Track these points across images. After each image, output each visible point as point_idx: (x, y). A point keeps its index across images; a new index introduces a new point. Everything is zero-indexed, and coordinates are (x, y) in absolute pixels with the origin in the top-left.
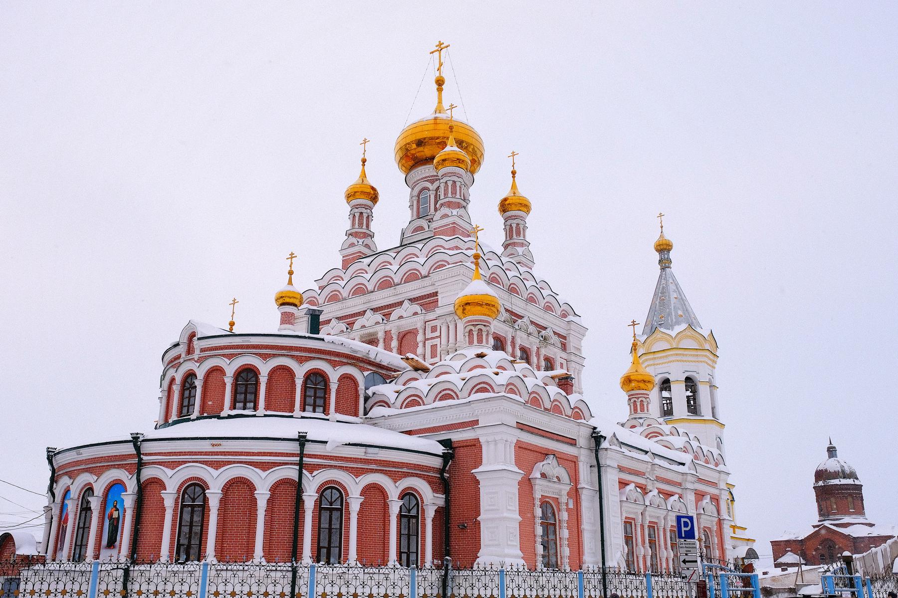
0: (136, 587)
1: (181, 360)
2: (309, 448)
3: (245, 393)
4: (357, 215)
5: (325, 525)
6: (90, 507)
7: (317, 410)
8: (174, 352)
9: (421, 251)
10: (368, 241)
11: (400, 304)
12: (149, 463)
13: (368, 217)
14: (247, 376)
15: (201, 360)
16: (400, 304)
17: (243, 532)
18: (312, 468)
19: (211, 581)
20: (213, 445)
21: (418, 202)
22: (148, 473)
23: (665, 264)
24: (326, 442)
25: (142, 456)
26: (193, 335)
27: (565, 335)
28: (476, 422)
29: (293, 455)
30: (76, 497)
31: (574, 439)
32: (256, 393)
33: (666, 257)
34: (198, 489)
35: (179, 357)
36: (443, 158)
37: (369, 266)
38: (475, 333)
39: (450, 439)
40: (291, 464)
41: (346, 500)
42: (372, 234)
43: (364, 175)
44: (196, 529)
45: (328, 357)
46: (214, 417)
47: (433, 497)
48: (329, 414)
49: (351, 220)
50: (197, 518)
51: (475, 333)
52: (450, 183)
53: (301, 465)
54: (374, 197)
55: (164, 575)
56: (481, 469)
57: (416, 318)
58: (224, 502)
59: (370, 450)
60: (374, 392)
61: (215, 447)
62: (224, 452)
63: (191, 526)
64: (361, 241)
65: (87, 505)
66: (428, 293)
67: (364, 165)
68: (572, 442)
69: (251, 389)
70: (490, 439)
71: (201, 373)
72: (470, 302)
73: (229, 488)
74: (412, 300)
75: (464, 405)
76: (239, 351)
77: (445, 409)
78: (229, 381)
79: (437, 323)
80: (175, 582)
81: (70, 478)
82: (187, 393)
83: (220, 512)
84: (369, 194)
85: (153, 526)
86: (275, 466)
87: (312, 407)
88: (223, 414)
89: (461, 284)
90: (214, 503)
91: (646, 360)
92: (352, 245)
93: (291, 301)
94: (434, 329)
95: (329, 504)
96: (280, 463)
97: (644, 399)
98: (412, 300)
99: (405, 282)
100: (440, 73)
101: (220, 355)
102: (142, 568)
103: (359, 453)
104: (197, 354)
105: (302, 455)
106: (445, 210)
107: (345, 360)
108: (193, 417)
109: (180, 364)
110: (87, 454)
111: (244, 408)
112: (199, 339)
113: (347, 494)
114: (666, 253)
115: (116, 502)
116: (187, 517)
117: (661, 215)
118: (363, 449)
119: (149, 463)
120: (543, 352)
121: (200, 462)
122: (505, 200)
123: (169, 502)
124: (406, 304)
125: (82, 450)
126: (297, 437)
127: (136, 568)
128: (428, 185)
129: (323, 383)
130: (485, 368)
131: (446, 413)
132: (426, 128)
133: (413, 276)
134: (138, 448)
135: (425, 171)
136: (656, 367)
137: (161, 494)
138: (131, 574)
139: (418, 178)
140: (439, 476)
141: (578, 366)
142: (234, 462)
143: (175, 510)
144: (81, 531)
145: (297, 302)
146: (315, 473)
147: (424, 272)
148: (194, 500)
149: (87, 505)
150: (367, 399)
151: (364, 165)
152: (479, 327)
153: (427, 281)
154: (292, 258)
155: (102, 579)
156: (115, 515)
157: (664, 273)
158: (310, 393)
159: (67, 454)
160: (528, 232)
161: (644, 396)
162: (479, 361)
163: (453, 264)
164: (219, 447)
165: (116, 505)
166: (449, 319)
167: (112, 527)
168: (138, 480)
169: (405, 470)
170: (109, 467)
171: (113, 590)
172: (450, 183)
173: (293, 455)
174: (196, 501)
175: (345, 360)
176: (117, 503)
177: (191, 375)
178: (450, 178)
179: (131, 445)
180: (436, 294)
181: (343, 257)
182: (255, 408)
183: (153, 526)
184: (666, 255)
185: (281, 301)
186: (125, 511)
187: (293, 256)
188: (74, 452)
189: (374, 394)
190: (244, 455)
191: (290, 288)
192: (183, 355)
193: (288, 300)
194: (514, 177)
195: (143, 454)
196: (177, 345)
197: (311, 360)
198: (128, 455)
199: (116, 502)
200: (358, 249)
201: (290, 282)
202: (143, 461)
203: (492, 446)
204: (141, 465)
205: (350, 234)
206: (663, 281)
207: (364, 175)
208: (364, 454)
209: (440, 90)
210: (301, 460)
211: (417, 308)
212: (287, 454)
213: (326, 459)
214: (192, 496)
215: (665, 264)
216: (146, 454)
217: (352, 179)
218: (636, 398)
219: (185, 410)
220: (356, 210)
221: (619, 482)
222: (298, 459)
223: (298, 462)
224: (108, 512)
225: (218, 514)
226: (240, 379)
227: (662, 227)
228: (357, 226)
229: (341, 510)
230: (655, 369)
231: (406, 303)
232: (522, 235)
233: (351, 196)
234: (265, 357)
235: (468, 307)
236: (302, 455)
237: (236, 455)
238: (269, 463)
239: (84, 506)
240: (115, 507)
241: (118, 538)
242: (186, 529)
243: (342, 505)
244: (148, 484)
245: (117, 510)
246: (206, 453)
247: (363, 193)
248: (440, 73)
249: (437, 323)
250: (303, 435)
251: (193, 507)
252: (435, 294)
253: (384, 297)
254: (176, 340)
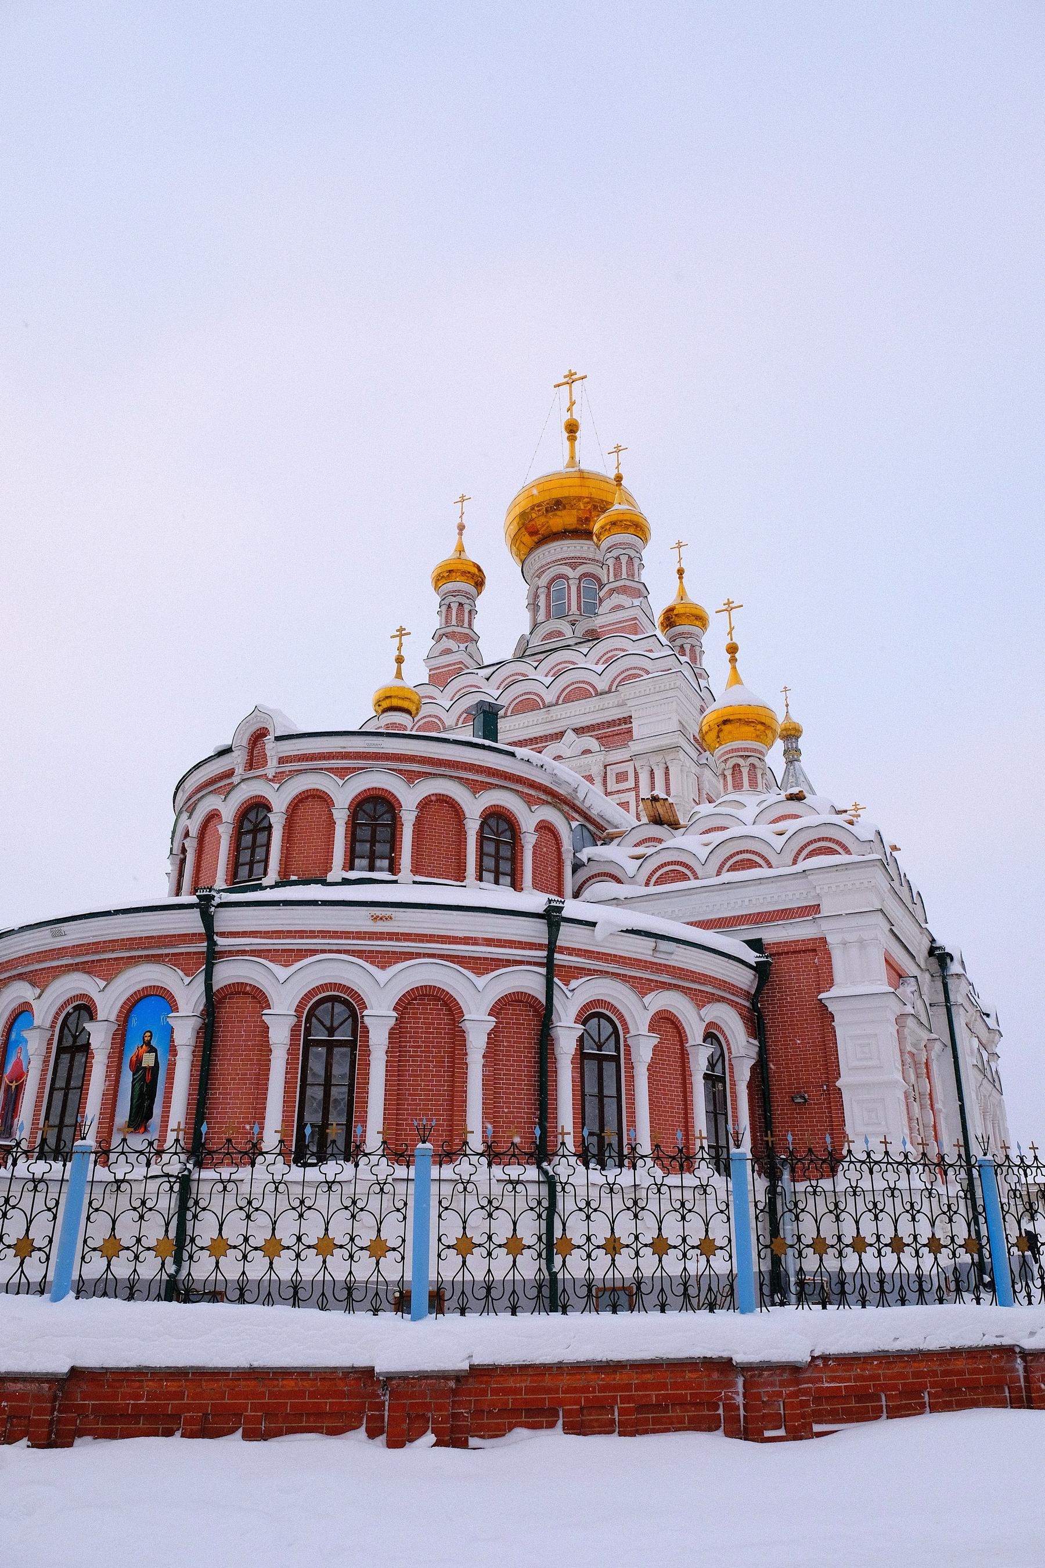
0: (808, 1229)
1: (235, 779)
2: (568, 935)
3: (373, 841)
4: (454, 607)
5: (591, 1088)
6: (89, 1044)
7: (501, 881)
8: (214, 767)
9: (585, 656)
10: (471, 647)
11: (559, 736)
12: (231, 953)
13: (470, 612)
14: (375, 809)
15: (279, 778)
16: (559, 736)
17: (439, 1100)
18: (572, 973)
19: (445, 1204)
20: (375, 918)
21: (548, 595)
22: (226, 973)
24: (594, 924)
25: (216, 938)
26: (259, 736)
28: (816, 908)
29: (531, 946)
30: (48, 1024)
32: (394, 843)
33: (794, 746)
34: (339, 1008)
35: (230, 774)
36: (614, 518)
37: (488, 679)
38: (745, 771)
39: (760, 940)
40: (529, 963)
41: (625, 1041)
42: (476, 638)
43: (461, 550)
44: (338, 1093)
45: (519, 787)
46: (316, 882)
47: (746, 1043)
48: (522, 889)
49: (444, 615)
50: (340, 1069)
51: (745, 771)
52: (624, 559)
53: (549, 964)
54: (478, 581)
55: (484, 1190)
56: (834, 992)
57: (588, 759)
58: (396, 1035)
59: (664, 945)
60: (590, 856)
61: (380, 923)
62: (397, 934)
63: (327, 1085)
64: (463, 646)
65: (75, 1041)
66: (610, 719)
67: (460, 534)
69: (383, 833)
70: (851, 937)
71: (280, 800)
72: (731, 718)
73: (405, 1008)
74: (579, 731)
75: (753, 882)
76: (361, 763)
77: (747, 886)
78: (341, 817)
79: (629, 767)
80: (637, 1211)
81: (33, 984)
82: (247, 839)
83: (391, 1056)
84: (473, 575)
85: (239, 1084)
86: (497, 967)
87: (493, 874)
88: (330, 878)
89: (675, 703)
90: (379, 1039)
92: (448, 651)
93: (405, 704)
94: (621, 777)
95: (595, 1047)
96: (508, 961)
98: (579, 731)
99: (564, 702)
100: (571, 415)
101: (322, 769)
102: (226, 1172)
103: (642, 948)
104: (271, 768)
105: (552, 948)
106: (617, 599)
107: (544, 797)
108: (265, 882)
109: (233, 787)
110: (75, 934)
111: (372, 868)
112: (278, 739)
113: (626, 1030)
114: (794, 740)
115: (148, 1034)
116: (317, 1066)
117: (786, 690)
118: (650, 943)
119: (231, 953)
121: (346, 952)
122: (671, 610)
123: (280, 1036)
124: (570, 735)
125: (65, 927)
126: (541, 910)
127: (207, 1174)
128: (567, 571)
129: (508, 834)
130: (801, 817)
131: (750, 891)
132: (568, 482)
133: (578, 693)
134: (208, 920)
135: (549, 552)
137: (264, 1017)
138: (194, 1186)
139: (549, 561)
140: (747, 1004)
142: (419, 955)
143: (291, 1052)
144: (59, 1096)
145: (413, 708)
146: (574, 983)
147: (602, 685)
148: (331, 1031)
149: (75, 1041)
150: (577, 867)
151: (460, 534)
152: (751, 760)
153: (610, 700)
154: (401, 635)
155: (445, 1204)
156: (148, 1060)
157: (792, 767)
158: (489, 848)
159: (27, 935)
160: (704, 657)
162: (794, 807)
163: (663, 671)
164: (386, 923)
165: (149, 1042)
166: (654, 759)
167: (142, 1087)
168: (208, 986)
169: (708, 989)
170: (133, 961)
171: (632, 1237)
172: (624, 559)
173: (531, 946)
174: (336, 1033)
175: (544, 797)
176: (151, 1036)
177: (258, 806)
178: (624, 552)
179: (196, 913)
180: (628, 720)
181: (430, 670)
182: (393, 869)
183: (239, 1084)
184: (794, 744)
185: (386, 704)
186: (173, 1051)
187: (403, 632)
188: (46, 931)
189: (589, 860)
190: (438, 942)
191: (398, 683)
192: (239, 770)
193: (395, 702)
194: (681, 578)
195: (217, 934)
196: (226, 751)
197: (490, 788)
198: (179, 935)
199: (148, 1034)
200: (459, 657)
201: (399, 675)
202: (217, 949)
203: (854, 952)
204: (212, 957)
205: (438, 637)
206: (790, 778)
207: (461, 550)
208: (651, 953)
209: (572, 439)
210: (550, 958)
211: (593, 744)
212: (520, 942)
213: (589, 958)
214: (328, 1023)
216: (222, 935)
217: (446, 553)
219: (243, 872)
220: (454, 599)
222: (545, 954)
223: (545, 961)
224: (129, 1055)
225: (387, 1061)
226: (361, 814)
227: (787, 705)
228: (454, 622)
229: (616, 1059)
231: (570, 735)
232: (698, 662)
233: (445, 575)
234: (411, 777)
235: (727, 728)
236: (552, 948)
237: (422, 941)
238: (487, 959)
239: (68, 1042)
240: (148, 1044)
241: (157, 1110)
242: (316, 1093)
243: (618, 1049)
244: (225, 997)
245: (152, 1050)
246: (359, 935)
247: (464, 573)
248: (571, 415)
249: (629, 767)
250: (558, 905)
251: (330, 1045)
252: (628, 720)
253: (526, 725)
254: (226, 741)
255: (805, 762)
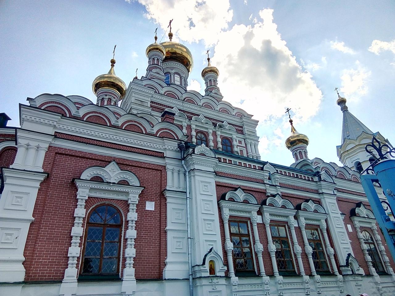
23: (345, 109)
27: (242, 126)
31: (161, 153)
68: (161, 155)
89: (133, 94)
91: (345, 156)
97: (301, 151)
120: (219, 133)
136: (351, 158)
141: (253, 142)
161: (301, 148)
215: (345, 109)
218: (295, 151)
221: (217, 185)
227: (338, 94)
230: (350, 159)
255: (350, 110)
